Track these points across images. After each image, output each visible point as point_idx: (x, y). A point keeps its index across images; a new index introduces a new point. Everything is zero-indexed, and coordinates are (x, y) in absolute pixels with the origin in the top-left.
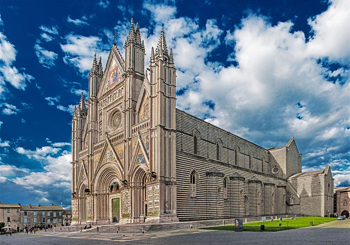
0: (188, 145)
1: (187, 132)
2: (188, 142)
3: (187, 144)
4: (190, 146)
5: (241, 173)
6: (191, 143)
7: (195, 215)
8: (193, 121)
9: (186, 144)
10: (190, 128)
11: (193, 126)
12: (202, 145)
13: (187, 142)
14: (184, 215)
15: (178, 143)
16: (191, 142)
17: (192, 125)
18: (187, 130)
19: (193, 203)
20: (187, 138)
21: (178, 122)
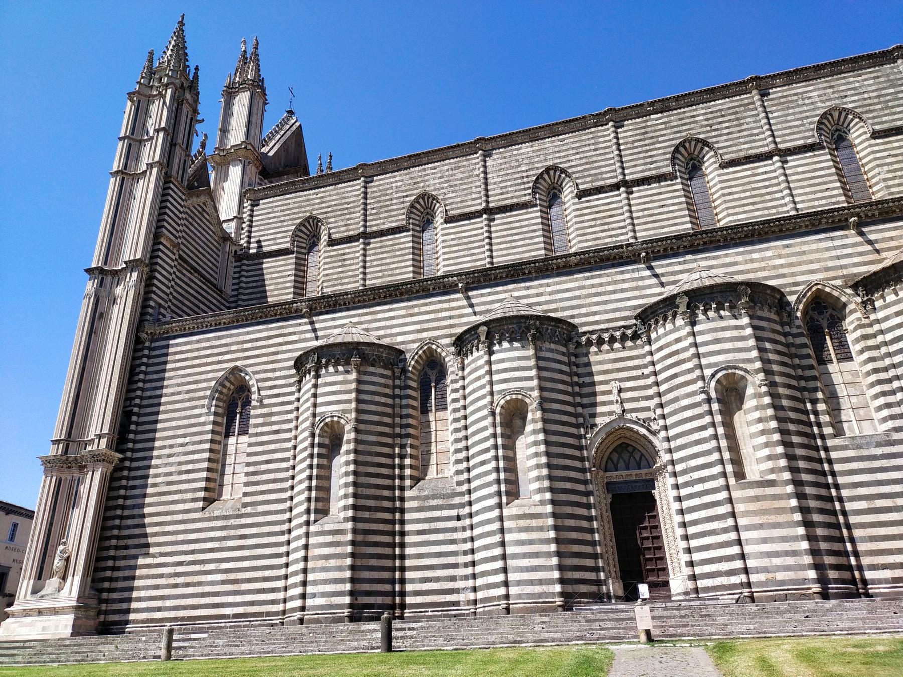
0: (385, 270)
1: (384, 223)
2: (388, 261)
3: (383, 268)
4: (397, 268)
5: (550, 294)
6: (400, 259)
7: (217, 600)
8: (406, 174)
9: (377, 272)
10: (396, 204)
11: (406, 191)
12: (453, 239)
13: (384, 261)
14: (158, 604)
15: (346, 281)
16: (398, 253)
17: (403, 191)
18: (380, 218)
19: (212, 534)
20: (381, 247)
21: (346, 211)
